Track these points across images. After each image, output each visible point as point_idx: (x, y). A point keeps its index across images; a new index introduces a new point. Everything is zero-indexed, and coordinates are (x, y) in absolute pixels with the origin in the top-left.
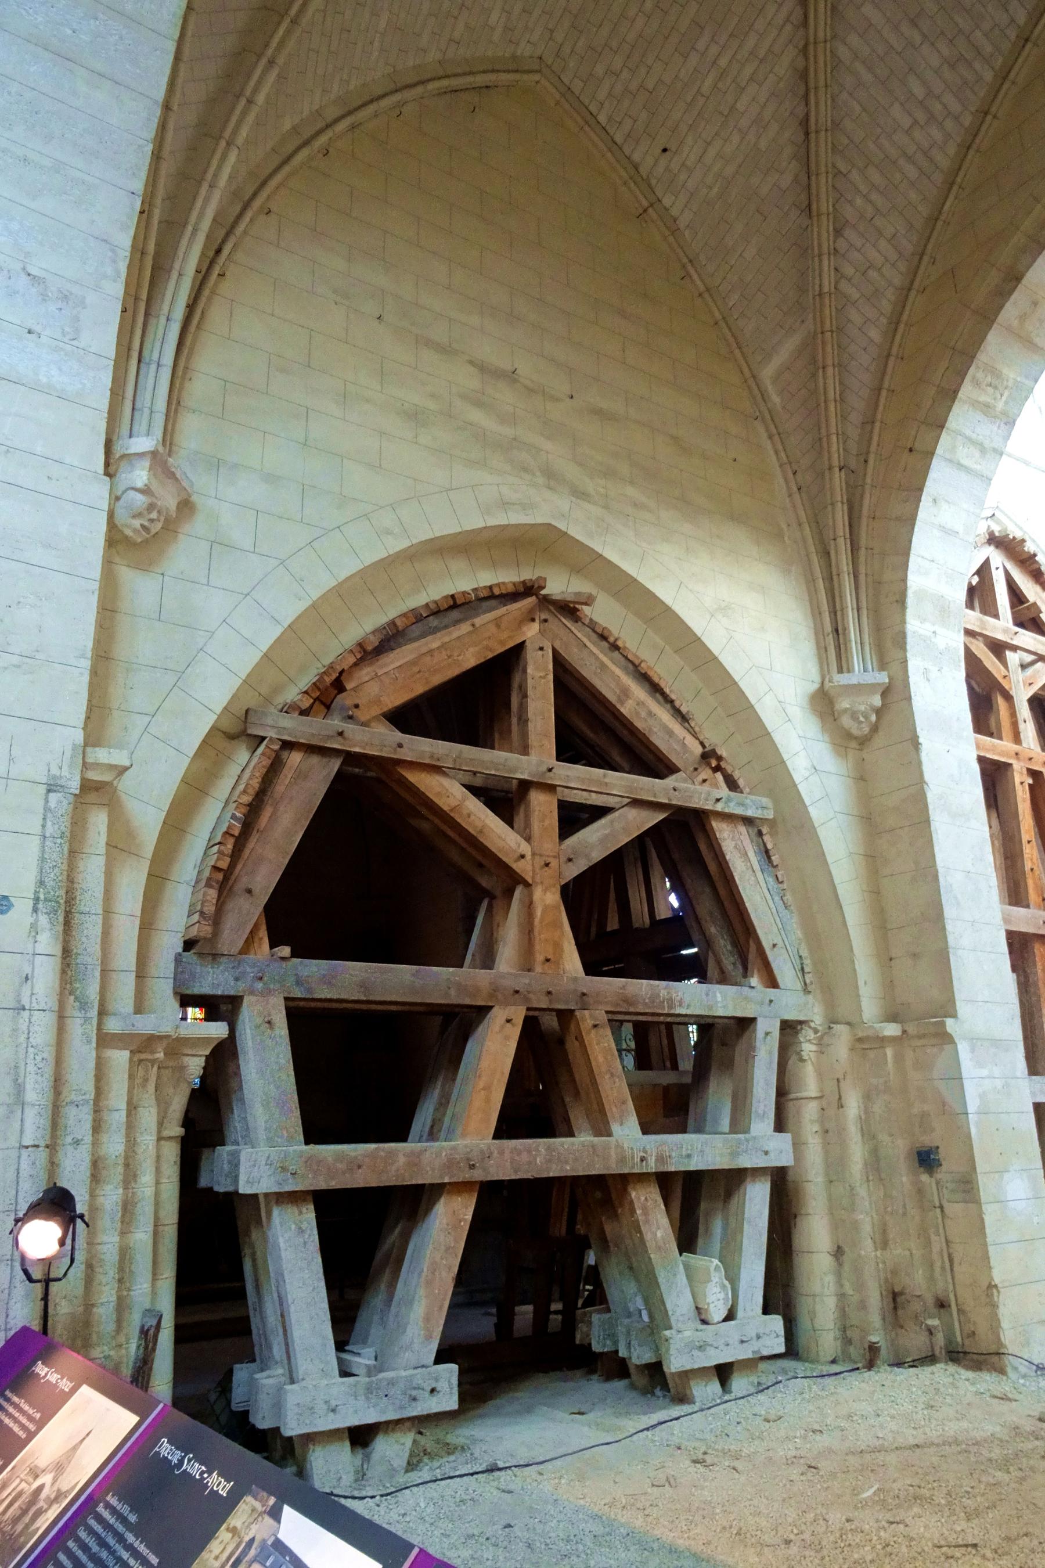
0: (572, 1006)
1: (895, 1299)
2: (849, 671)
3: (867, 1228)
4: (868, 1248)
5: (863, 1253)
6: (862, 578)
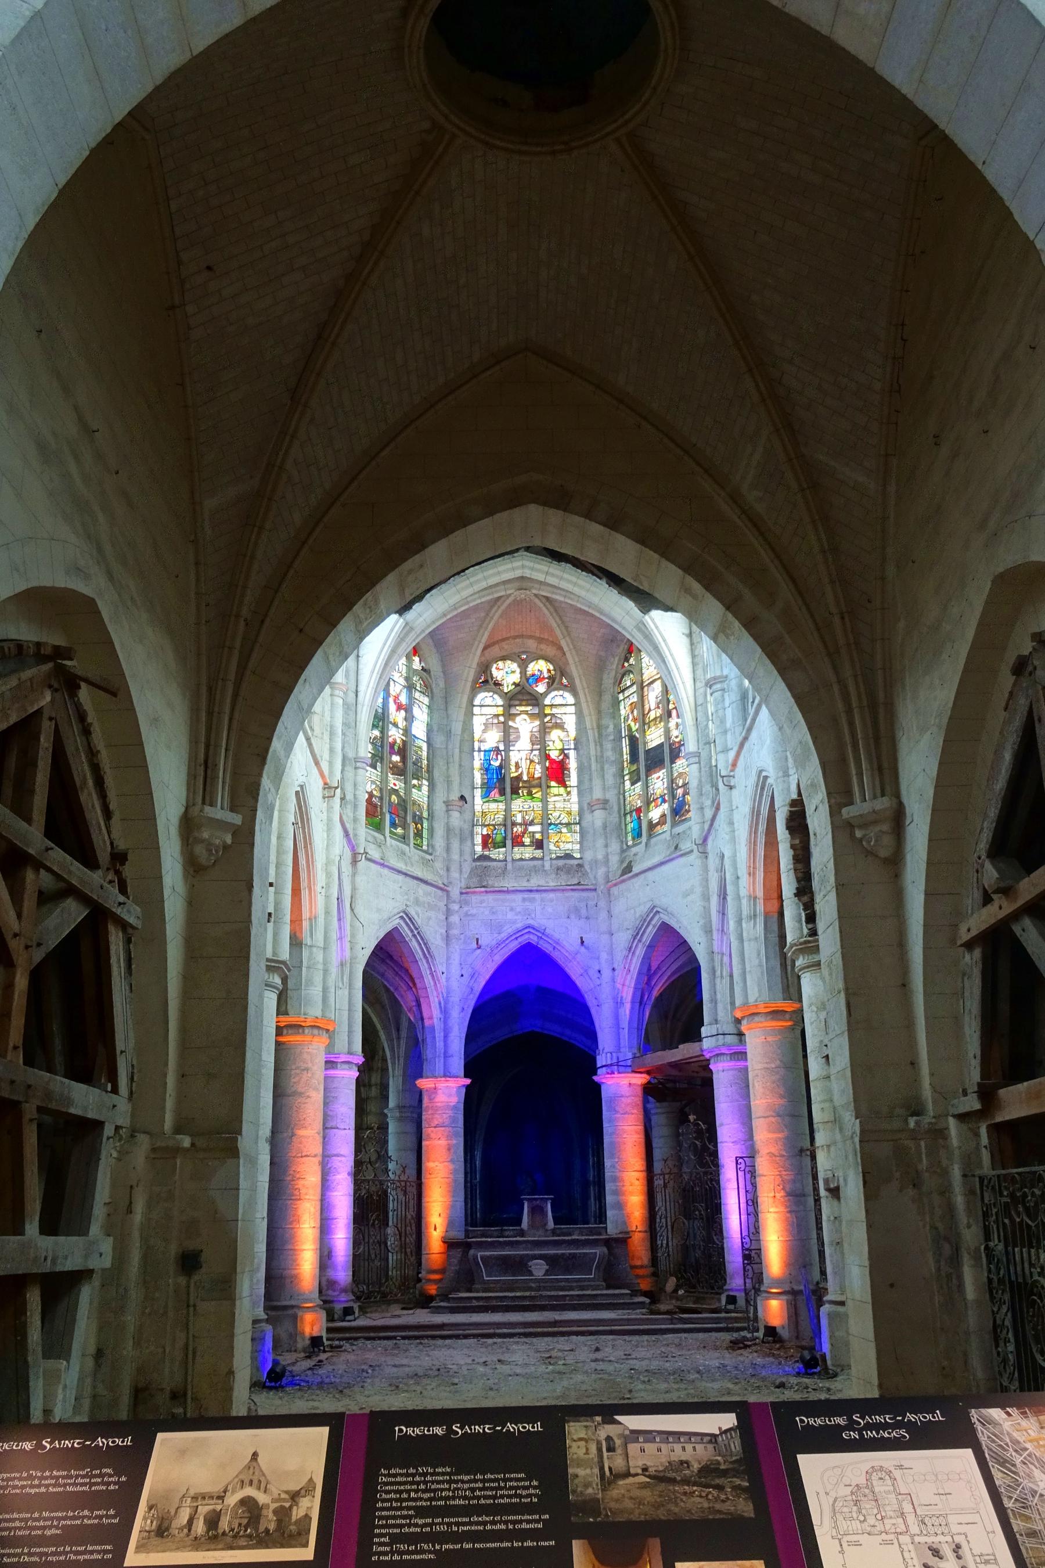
0: (21, 1099)
4: (128, 1349)
6: (235, 723)
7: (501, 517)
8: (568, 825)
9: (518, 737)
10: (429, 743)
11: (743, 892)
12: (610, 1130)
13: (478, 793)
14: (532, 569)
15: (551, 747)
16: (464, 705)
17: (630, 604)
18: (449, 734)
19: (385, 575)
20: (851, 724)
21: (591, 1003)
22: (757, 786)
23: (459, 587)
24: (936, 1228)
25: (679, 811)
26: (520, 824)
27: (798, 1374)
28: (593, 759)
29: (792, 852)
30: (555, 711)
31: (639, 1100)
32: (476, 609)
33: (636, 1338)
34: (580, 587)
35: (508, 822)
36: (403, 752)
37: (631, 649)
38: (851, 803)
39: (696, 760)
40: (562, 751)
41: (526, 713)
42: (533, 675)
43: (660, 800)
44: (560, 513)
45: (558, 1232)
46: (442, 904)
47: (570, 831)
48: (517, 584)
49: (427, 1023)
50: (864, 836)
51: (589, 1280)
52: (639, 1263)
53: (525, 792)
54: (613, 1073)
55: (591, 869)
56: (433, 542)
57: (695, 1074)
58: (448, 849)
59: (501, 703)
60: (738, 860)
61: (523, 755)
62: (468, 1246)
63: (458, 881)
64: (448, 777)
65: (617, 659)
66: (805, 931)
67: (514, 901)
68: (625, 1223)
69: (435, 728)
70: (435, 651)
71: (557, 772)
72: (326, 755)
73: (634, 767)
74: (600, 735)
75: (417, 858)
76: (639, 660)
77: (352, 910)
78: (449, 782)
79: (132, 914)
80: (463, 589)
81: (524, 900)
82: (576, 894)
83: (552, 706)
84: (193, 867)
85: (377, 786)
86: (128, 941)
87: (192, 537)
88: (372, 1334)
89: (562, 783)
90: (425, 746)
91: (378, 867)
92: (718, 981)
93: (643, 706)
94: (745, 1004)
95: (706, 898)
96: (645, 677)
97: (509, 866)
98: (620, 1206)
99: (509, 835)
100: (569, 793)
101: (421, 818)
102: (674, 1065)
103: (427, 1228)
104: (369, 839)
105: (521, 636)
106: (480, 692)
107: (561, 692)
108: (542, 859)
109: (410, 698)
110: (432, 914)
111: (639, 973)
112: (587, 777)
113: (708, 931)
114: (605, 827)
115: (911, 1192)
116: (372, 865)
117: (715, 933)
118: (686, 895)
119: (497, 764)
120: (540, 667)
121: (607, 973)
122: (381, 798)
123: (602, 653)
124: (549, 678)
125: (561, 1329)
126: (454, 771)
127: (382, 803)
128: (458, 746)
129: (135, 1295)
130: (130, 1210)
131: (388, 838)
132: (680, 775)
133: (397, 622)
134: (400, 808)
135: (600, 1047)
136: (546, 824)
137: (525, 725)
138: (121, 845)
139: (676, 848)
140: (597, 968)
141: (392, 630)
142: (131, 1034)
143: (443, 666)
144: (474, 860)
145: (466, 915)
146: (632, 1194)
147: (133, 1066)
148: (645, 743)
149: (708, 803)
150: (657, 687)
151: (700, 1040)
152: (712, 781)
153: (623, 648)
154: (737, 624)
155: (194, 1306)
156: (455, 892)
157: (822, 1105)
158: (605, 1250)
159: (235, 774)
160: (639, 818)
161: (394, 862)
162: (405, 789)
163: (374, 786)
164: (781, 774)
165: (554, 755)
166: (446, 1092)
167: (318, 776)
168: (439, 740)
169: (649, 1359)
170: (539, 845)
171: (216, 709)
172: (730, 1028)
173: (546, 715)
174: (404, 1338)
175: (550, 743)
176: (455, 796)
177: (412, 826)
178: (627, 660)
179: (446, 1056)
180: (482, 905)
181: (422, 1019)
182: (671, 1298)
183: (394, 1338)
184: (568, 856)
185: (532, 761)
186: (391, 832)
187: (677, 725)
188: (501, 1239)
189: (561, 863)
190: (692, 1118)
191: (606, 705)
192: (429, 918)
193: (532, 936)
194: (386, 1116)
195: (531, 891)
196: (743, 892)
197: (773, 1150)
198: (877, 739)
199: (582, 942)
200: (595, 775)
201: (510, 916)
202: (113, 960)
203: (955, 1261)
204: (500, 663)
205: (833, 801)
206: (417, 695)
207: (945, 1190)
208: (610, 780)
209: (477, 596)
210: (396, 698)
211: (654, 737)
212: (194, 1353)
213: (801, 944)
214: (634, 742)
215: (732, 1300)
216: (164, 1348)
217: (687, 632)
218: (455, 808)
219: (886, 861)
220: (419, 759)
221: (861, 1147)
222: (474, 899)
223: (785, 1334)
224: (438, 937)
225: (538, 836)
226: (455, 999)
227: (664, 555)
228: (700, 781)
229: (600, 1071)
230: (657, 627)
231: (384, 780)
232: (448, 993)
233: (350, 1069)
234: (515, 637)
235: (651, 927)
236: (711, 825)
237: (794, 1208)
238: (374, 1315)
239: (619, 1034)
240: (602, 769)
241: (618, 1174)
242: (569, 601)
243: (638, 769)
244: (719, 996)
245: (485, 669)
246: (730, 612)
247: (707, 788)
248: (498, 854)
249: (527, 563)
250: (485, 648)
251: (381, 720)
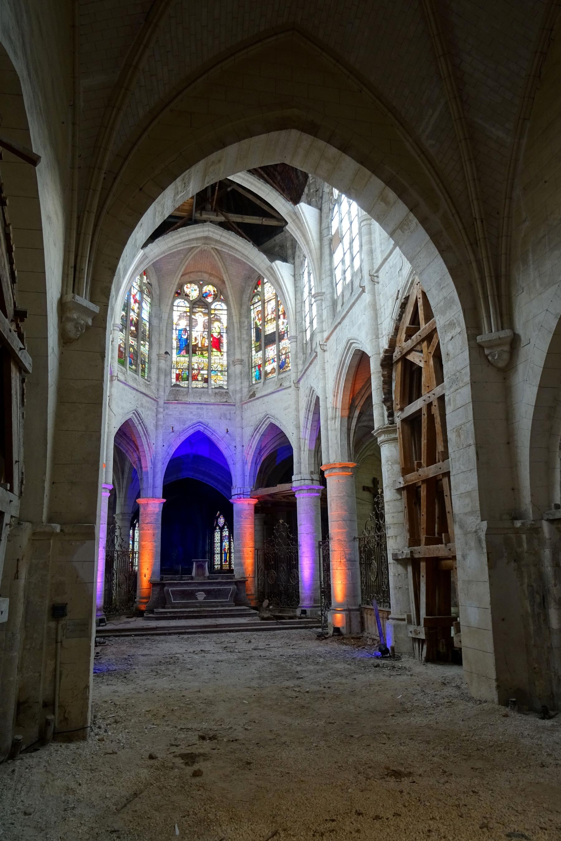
1: (21, 705)
2: (78, 294)
3: (17, 661)
5: (12, 679)
7: (274, 135)
8: (221, 371)
9: (197, 324)
11: (329, 405)
12: (238, 527)
13: (174, 352)
14: (214, 232)
15: (214, 331)
17: (265, 257)
18: (160, 319)
19: (199, 161)
20: (484, 286)
21: (230, 462)
22: (346, 348)
23: (174, 238)
24: (532, 586)
25: (282, 366)
26: (196, 369)
27: (377, 657)
28: (236, 338)
29: (382, 379)
30: (216, 312)
31: (253, 512)
32: (179, 252)
33: (263, 634)
34: (240, 245)
35: (190, 368)
36: (137, 325)
37: (259, 282)
38: (480, 333)
39: (295, 340)
40: (220, 333)
41: (201, 312)
42: (206, 293)
43: (272, 361)
44: (312, 137)
45: (211, 577)
46: (154, 408)
47: (222, 375)
48: (203, 241)
49: (144, 470)
50: (490, 353)
51: (226, 602)
52: (250, 593)
53: (200, 353)
54: (241, 498)
55: (233, 395)
56: (231, 143)
57: (280, 500)
58: (158, 380)
59: (188, 305)
60: (327, 389)
61: (199, 333)
62: (164, 585)
63: (163, 396)
64: (159, 342)
65: (251, 288)
66: (386, 422)
67: (192, 409)
68: (244, 573)
69: (153, 315)
70: (155, 274)
71: (217, 344)
73: (258, 344)
74: (240, 326)
75: (142, 382)
76: (263, 289)
77: (109, 406)
78: (160, 344)
79: (27, 360)
80: (176, 239)
81: (198, 408)
82: (225, 407)
83: (215, 309)
84: (65, 339)
86: (23, 381)
87: (72, 103)
88: (118, 634)
89: (219, 349)
90: (148, 324)
92: (302, 453)
93: (264, 313)
94: (328, 463)
95: (297, 410)
96: (266, 298)
97: (190, 390)
98: (241, 564)
99: (189, 375)
100: (222, 355)
101: (145, 362)
102: (271, 495)
103: (140, 576)
105: (201, 272)
106: (177, 299)
107: (220, 303)
108: (207, 388)
109: (142, 298)
110: (149, 412)
111: (256, 448)
112: (232, 347)
113: (298, 427)
114: (241, 373)
115: (513, 564)
116: (121, 384)
117: (302, 429)
118: (285, 409)
119: (185, 337)
120: (209, 289)
121: (239, 448)
122: (125, 349)
123: (243, 284)
124: (214, 295)
125: (221, 629)
126: (163, 338)
129: (19, 637)
130: (16, 577)
131: (128, 371)
132: (284, 348)
135: (234, 485)
136: (210, 370)
137: (200, 318)
138: (20, 307)
139: (281, 385)
140: (234, 445)
142: (22, 450)
143: (159, 283)
144: (172, 386)
145: (167, 414)
146: (247, 558)
147: (22, 473)
148: (265, 332)
149: (301, 362)
150: (273, 303)
151: (290, 481)
152: (303, 351)
153: (255, 282)
154: (415, 221)
155: (61, 642)
156: (161, 402)
157: (393, 515)
158: (236, 587)
159: (93, 279)
160: (260, 369)
161: (131, 383)
163: (121, 342)
164: (374, 337)
165: (215, 335)
166: (153, 506)
168: (155, 322)
169: (281, 647)
170: (206, 381)
171: (83, 231)
172: (308, 477)
173: (212, 314)
174: (136, 635)
175: (214, 329)
176: (163, 352)
177: (141, 365)
178: (256, 288)
179: (154, 487)
180: (175, 410)
181: (141, 468)
182: (266, 610)
183: (130, 635)
184: (221, 387)
185: (203, 337)
186: (130, 367)
187: (283, 323)
188: (182, 582)
189: (217, 391)
190: (281, 521)
191: (244, 311)
192: (148, 415)
193: (201, 427)
194: (114, 518)
195: (201, 404)
196: (329, 405)
197: (340, 538)
198: (499, 296)
199: (228, 431)
200: (237, 346)
201: (190, 416)
202: (13, 392)
203: (544, 604)
204: (189, 285)
205: (469, 332)
206: (145, 296)
207: (538, 563)
208: (245, 350)
209: (182, 245)
210: (134, 296)
211: (270, 329)
212: (61, 675)
213: (384, 428)
214: (258, 332)
215: (304, 612)
216: (39, 672)
217: (293, 274)
219: (500, 370)
221: (486, 537)
222: (171, 405)
223: (344, 631)
224: (152, 424)
225: (206, 376)
226: (160, 457)
227: (374, 172)
228: (296, 351)
229: (233, 497)
230: (278, 270)
231: (127, 340)
232: (156, 454)
233: (106, 492)
234: (198, 272)
235: (264, 425)
236: (305, 373)
237: (350, 567)
238: (114, 622)
239: (244, 479)
240: (241, 344)
241: (241, 549)
242: (230, 253)
243: (260, 345)
244: (302, 460)
245: (181, 286)
246: (413, 213)
247: (300, 355)
248: (184, 384)
249: (210, 229)
250: (182, 275)
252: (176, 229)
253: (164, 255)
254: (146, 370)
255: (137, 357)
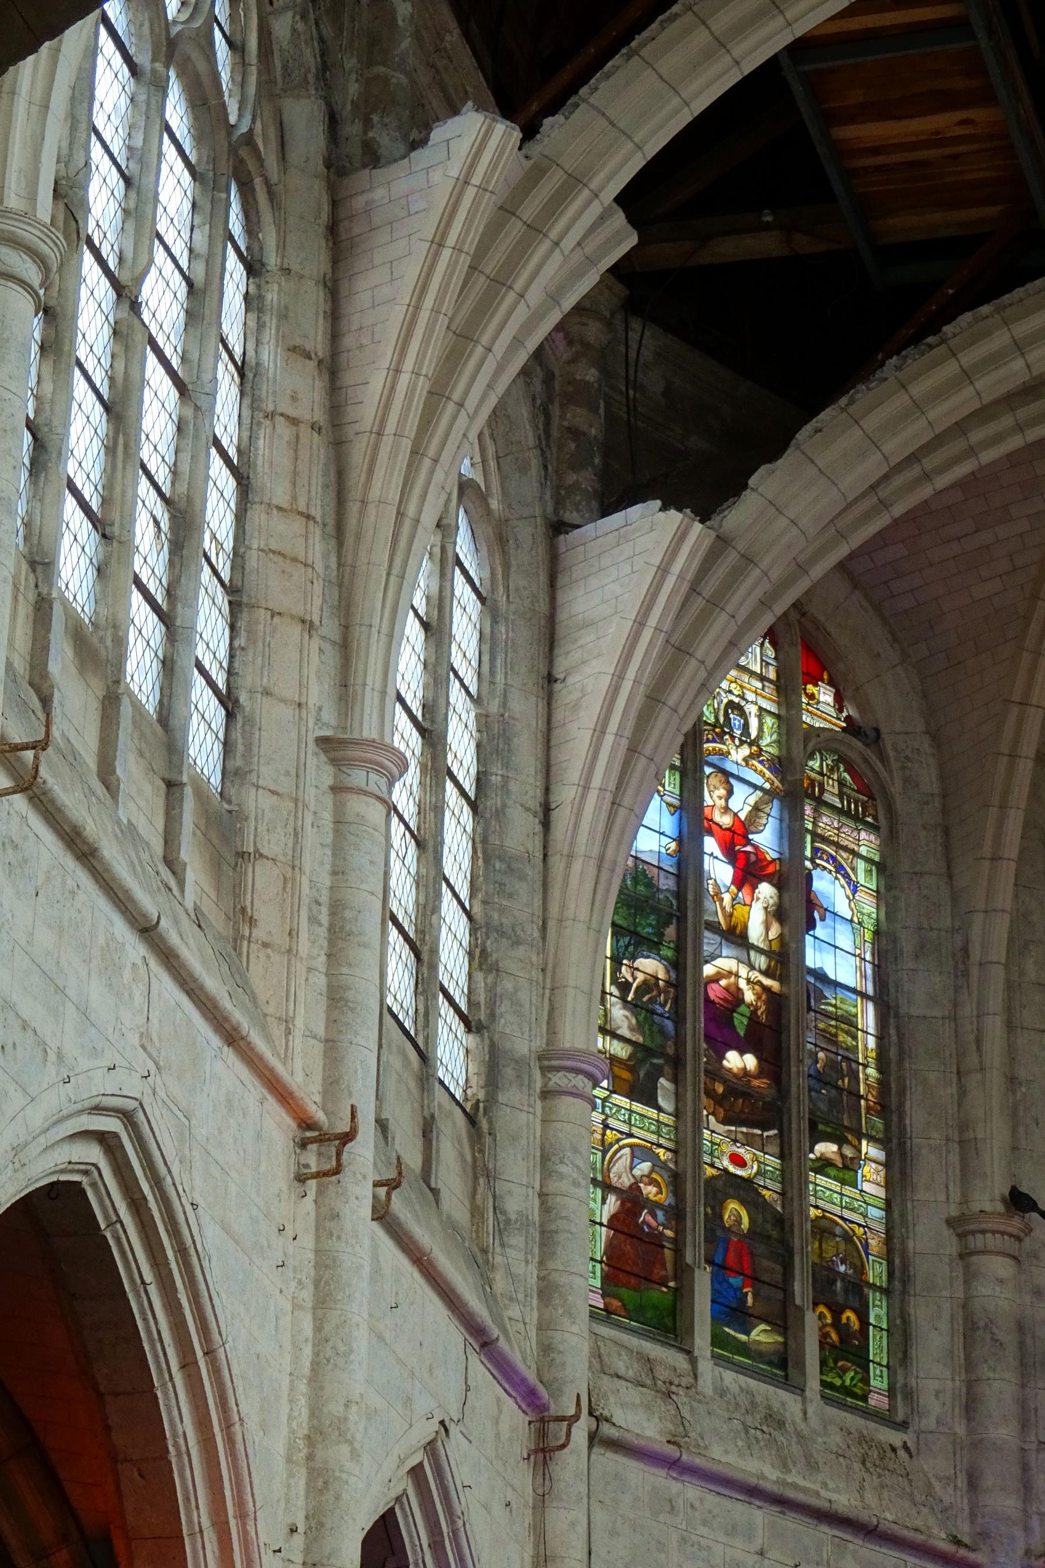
10: (884, 1000)
16: (1012, 848)
23: (918, 389)
58: (971, 1404)
72: (310, 1015)
75: (836, 1439)
78: (967, 1146)
85: (658, 1164)
90: (868, 1018)
91: (658, 1478)
104: (621, 1364)
109: (792, 833)
116: (633, 1470)
122: (677, 1214)
126: (988, 1100)
127: (680, 1232)
128: (995, 1001)
131: (706, 1367)
133: (680, 537)
134: (761, 1249)
141: (663, 570)
161: (726, 1454)
162: (784, 1176)
163: (645, 1167)
167: (254, 1092)
168: (923, 989)
176: (988, 1198)
186: (718, 1340)
209: (1006, 421)
218: (992, 1241)
220: (845, 1063)
231: (686, 1143)
251: (659, 913)
252: (933, 326)
253: (882, 521)
254: (877, 1346)
255: (786, 1259)
